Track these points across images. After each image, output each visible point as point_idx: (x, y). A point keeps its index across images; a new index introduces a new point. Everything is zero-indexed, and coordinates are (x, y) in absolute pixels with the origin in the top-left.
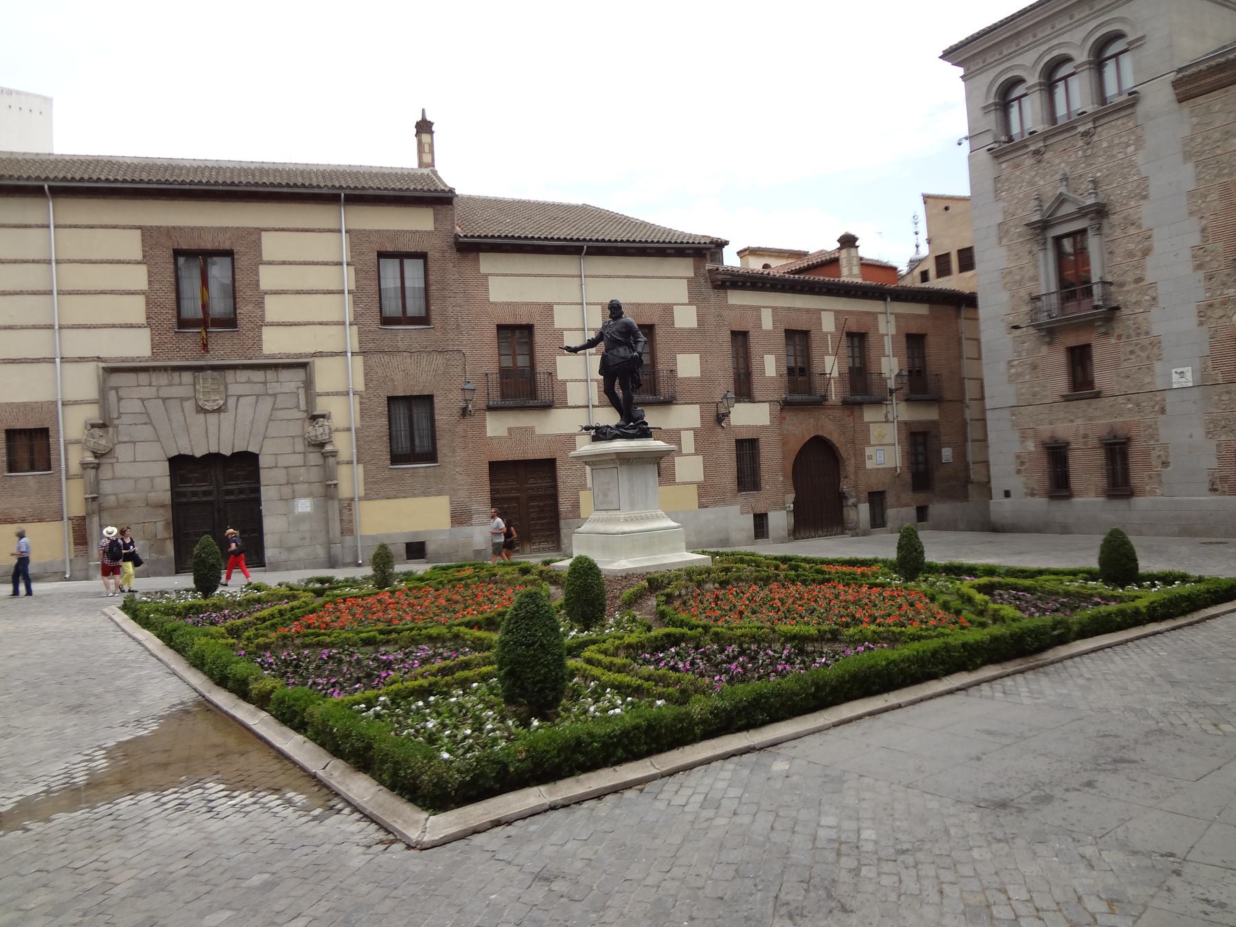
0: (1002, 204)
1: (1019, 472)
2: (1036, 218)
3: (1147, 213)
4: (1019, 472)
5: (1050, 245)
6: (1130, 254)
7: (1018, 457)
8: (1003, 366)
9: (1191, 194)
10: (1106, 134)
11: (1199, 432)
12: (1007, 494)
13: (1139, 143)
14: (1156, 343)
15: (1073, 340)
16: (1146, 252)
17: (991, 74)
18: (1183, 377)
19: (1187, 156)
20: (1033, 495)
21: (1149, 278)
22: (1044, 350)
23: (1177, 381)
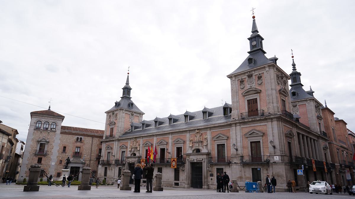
0: (34, 136)
1: (25, 173)
2: (39, 140)
3: (54, 144)
4: (25, 173)
5: (40, 144)
6: (50, 148)
7: (26, 171)
8: (27, 158)
9: (59, 144)
10: (51, 133)
11: (54, 170)
12: (22, 177)
13: (55, 136)
14: (51, 159)
15: (40, 157)
16: (52, 148)
17: (37, 119)
18: (53, 164)
19: (60, 140)
20: (27, 177)
21: (52, 152)
22: (35, 157)
23: (52, 164)
